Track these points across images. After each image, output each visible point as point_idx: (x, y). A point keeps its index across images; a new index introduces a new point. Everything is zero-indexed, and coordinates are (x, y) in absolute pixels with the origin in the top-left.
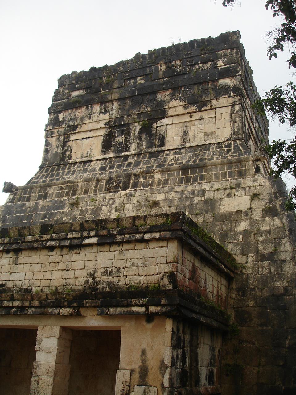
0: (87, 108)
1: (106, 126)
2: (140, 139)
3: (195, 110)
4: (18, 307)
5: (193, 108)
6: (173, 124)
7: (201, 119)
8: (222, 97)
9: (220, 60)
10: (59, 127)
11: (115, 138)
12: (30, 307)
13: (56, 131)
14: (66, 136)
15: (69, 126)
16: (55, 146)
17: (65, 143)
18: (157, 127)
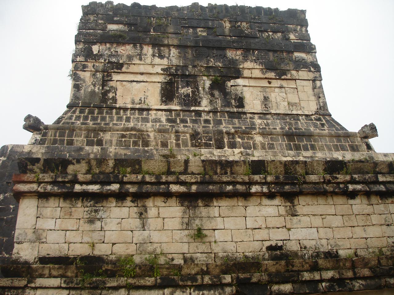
0: (135, 46)
1: (165, 73)
2: (212, 95)
3: (274, 77)
4: (331, 280)
5: (272, 75)
6: (250, 86)
7: (281, 87)
8: (302, 70)
9: (291, 33)
10: (96, 61)
11: (178, 88)
12: (356, 278)
13: (90, 65)
14: (106, 74)
15: (110, 62)
16: (90, 83)
17: (104, 83)
18: (232, 86)
